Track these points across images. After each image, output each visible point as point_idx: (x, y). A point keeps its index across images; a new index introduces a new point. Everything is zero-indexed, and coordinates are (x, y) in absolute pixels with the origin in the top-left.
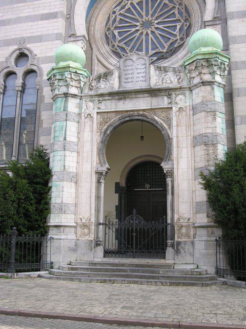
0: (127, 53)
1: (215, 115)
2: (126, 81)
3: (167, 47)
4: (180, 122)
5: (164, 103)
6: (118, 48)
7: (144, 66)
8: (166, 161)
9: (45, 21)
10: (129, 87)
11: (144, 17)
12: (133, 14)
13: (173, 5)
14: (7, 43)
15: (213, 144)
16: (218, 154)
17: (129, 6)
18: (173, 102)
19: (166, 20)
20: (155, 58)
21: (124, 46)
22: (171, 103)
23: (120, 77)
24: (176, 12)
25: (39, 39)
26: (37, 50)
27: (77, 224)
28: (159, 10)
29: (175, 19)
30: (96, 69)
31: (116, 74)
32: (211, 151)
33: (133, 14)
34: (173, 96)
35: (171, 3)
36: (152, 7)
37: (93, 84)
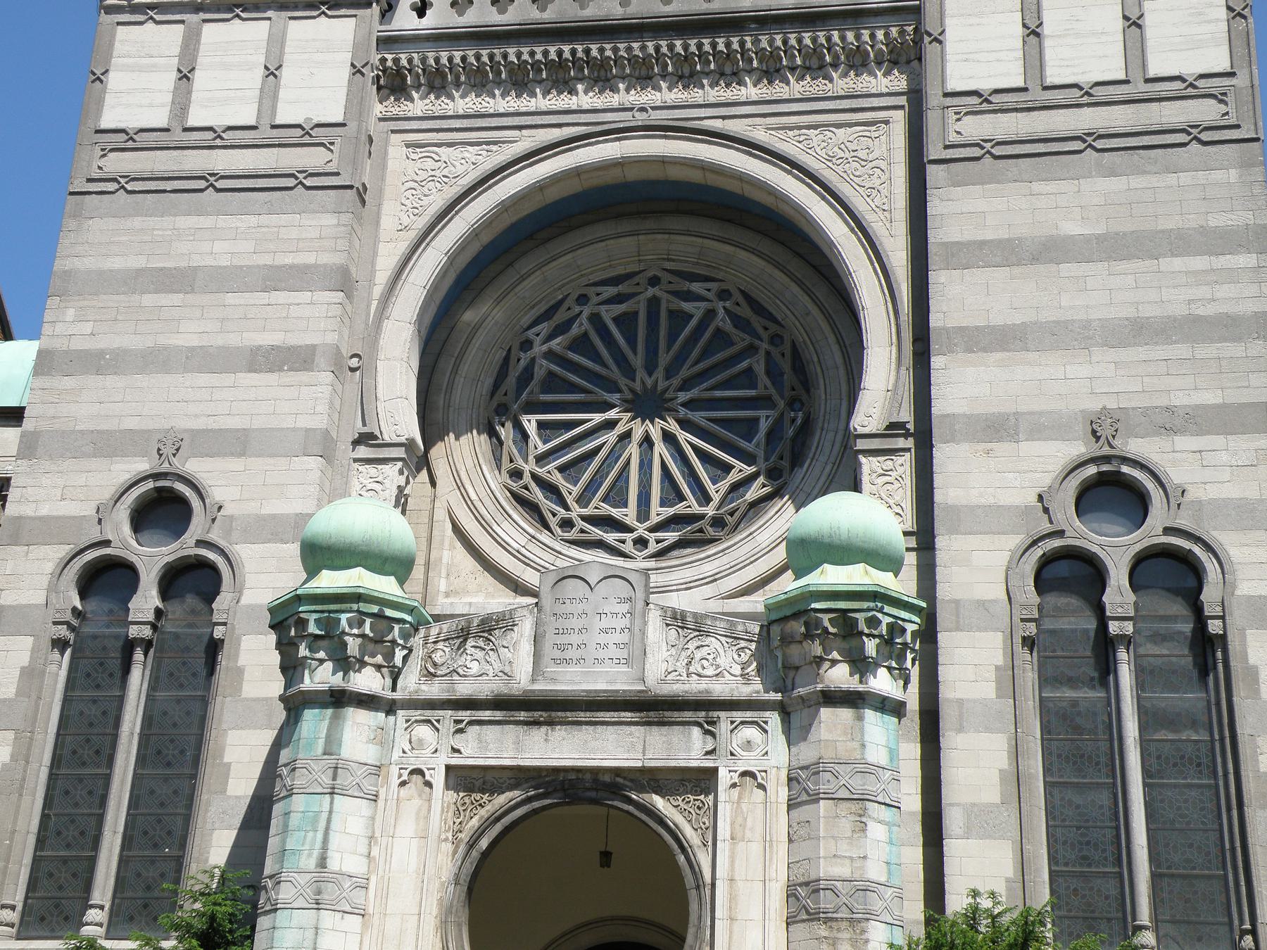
0: (567, 508)
1: (862, 814)
2: (557, 654)
3: (716, 498)
4: (743, 826)
5: (689, 750)
6: (533, 485)
7: (625, 607)
9: (262, 375)
10: (571, 680)
11: (641, 374)
12: (597, 358)
13: (748, 339)
14: (107, 444)
15: (851, 920)
17: (586, 325)
18: (721, 751)
20: (671, 536)
21: (558, 479)
23: (537, 640)
24: (760, 369)
25: (237, 443)
26: (226, 485)
28: (696, 353)
29: (753, 393)
30: (444, 561)
31: (526, 627)
33: (597, 358)
34: (724, 727)
36: (672, 338)
37: (437, 657)
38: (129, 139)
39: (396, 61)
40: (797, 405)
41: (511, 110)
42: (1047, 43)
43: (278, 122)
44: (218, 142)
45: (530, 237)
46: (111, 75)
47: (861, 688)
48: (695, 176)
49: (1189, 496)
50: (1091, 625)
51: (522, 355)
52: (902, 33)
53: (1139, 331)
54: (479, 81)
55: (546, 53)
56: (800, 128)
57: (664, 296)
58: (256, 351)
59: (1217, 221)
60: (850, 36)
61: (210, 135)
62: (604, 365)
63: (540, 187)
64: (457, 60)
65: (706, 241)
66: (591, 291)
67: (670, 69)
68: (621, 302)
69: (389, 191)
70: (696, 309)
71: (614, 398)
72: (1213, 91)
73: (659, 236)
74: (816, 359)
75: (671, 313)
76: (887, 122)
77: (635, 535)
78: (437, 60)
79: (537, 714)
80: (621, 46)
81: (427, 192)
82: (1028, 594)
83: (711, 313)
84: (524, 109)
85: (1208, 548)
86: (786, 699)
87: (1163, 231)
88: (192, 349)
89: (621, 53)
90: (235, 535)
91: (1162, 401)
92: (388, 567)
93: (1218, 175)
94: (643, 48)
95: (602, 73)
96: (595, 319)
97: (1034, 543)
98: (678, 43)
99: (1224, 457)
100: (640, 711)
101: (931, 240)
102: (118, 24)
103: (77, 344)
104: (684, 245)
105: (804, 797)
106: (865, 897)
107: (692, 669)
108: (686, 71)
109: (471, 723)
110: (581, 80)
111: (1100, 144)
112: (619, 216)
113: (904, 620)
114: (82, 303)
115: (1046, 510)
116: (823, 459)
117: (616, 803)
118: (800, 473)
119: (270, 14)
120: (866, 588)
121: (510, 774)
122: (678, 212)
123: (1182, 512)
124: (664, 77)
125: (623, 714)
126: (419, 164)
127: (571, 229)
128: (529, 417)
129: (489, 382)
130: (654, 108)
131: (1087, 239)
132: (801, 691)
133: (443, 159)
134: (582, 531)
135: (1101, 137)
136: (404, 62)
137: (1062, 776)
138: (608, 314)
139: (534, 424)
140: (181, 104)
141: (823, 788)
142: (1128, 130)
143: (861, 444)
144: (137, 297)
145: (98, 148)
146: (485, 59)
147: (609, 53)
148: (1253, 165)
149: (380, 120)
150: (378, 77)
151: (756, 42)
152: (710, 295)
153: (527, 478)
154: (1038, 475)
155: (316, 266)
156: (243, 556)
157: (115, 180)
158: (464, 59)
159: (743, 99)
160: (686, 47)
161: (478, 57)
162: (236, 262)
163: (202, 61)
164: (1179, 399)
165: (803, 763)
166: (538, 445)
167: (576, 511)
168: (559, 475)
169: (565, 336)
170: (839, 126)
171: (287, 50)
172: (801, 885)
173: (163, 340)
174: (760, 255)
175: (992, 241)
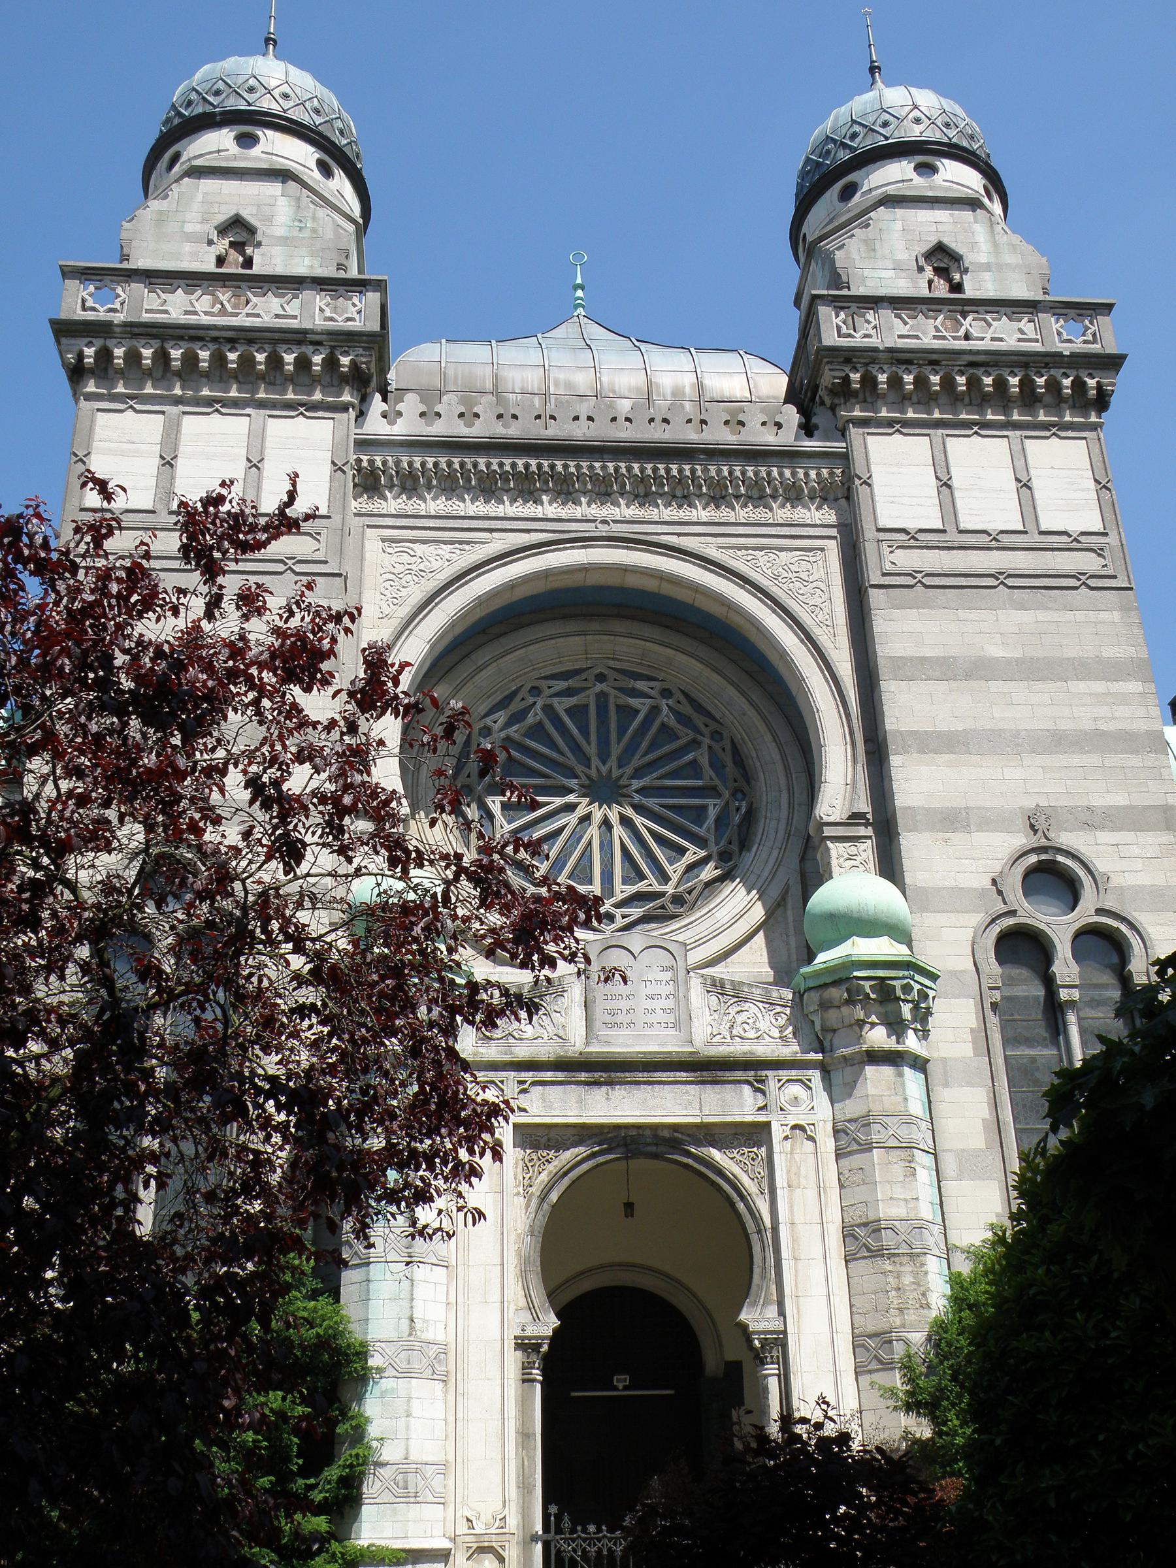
2: (608, 1019)
3: (675, 878)
4: (798, 1174)
5: (742, 1106)
7: (668, 975)
8: (754, 1304)
11: (595, 762)
12: (553, 745)
13: (692, 735)
15: (911, 1255)
16: (929, 1289)
18: (772, 1107)
19: (668, 782)
20: (636, 912)
22: (764, 1108)
24: (704, 761)
27: (454, 1540)
28: (644, 745)
29: (699, 783)
32: (907, 1280)
33: (553, 745)
34: (772, 1085)
35: (685, 726)
36: (622, 731)
40: (739, 796)
41: (481, 514)
42: (957, 494)
45: (483, 631)
47: (900, 1048)
50: (1040, 992)
52: (832, 474)
53: (1059, 741)
54: (450, 485)
55: (514, 465)
56: (747, 549)
57: (613, 692)
59: (1108, 653)
60: (787, 473)
62: (562, 753)
63: (512, 586)
64: (430, 465)
65: (648, 644)
66: (544, 684)
67: (628, 488)
69: (368, 582)
70: (642, 706)
71: (573, 783)
75: (618, 706)
76: (822, 550)
78: (410, 464)
79: (597, 1075)
80: (584, 464)
81: (406, 584)
82: (992, 966)
83: (655, 710)
84: (493, 514)
86: (828, 1060)
87: (1068, 659)
89: (585, 470)
93: (1105, 615)
94: (604, 468)
95: (565, 487)
96: (548, 709)
97: (993, 921)
98: (636, 466)
100: (694, 1071)
101: (879, 654)
102: (98, 410)
104: (628, 646)
105: (855, 1147)
106: (921, 1234)
107: (735, 1032)
108: (642, 491)
109: (534, 1084)
110: (546, 491)
111: (1010, 582)
112: (565, 617)
113: (927, 987)
115: (1000, 893)
116: (769, 844)
117: (675, 1157)
118: (748, 857)
119: (248, 411)
120: (900, 959)
121: (571, 1131)
122: (619, 616)
123: (1109, 896)
124: (622, 495)
125: (678, 1074)
126: (395, 558)
127: (521, 626)
128: (493, 798)
130: (615, 522)
131: (1009, 661)
132: (846, 1051)
133: (419, 554)
135: (1010, 576)
136: (379, 464)
137: (1027, 1124)
138: (561, 705)
139: (499, 805)
141: (875, 1138)
142: (1031, 572)
143: (828, 831)
146: (457, 466)
147: (572, 470)
148: (1130, 609)
151: (706, 470)
152: (652, 693)
158: (436, 465)
160: (642, 470)
161: (449, 464)
164: (1097, 801)
165: (849, 1117)
169: (522, 724)
170: (781, 549)
171: (267, 444)
172: (858, 1226)
175: (930, 658)
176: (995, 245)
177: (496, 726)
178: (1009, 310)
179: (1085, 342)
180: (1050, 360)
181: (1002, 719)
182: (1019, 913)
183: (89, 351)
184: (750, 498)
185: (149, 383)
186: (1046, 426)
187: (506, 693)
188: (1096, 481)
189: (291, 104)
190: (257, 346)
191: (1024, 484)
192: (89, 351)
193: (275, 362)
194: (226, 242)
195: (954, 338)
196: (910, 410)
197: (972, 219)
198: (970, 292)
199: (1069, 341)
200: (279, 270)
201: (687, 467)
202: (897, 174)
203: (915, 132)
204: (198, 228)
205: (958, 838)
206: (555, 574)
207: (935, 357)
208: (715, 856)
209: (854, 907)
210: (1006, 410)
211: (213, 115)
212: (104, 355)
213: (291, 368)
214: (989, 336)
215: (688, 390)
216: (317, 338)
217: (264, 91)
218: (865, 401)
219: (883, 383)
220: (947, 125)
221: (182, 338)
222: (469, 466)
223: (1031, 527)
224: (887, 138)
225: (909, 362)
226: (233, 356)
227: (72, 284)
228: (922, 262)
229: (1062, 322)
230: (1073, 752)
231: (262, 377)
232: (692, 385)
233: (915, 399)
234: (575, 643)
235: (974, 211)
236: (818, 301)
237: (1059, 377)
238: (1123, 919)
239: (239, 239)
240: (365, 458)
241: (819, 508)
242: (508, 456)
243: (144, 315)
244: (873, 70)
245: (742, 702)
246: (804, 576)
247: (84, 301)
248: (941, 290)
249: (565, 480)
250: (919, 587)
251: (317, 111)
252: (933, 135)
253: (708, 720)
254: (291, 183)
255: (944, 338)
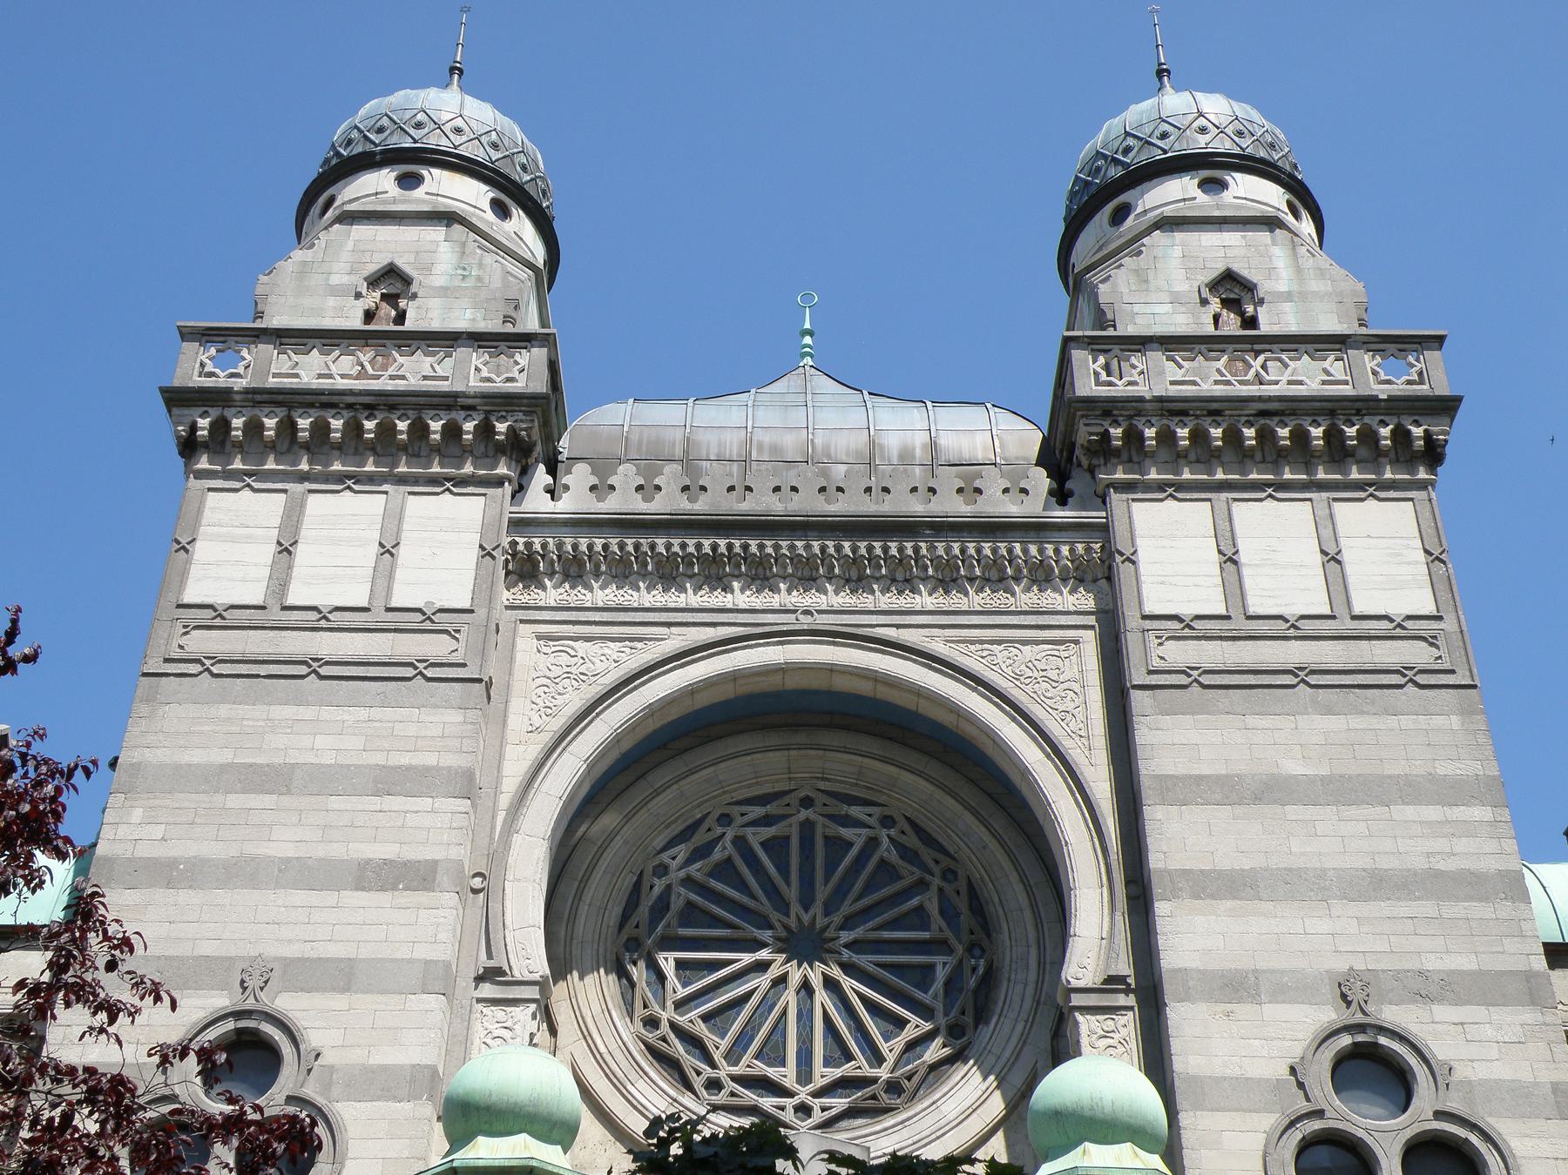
0: (713, 1065)
3: (891, 1058)
6: (672, 1037)
11: (795, 908)
12: (743, 887)
13: (918, 873)
17: (730, 849)
19: (886, 935)
20: (839, 1103)
21: (701, 1029)
24: (933, 907)
25: (341, 976)
29: (926, 935)
33: (743, 887)
36: (830, 869)
38: (217, 617)
39: (528, 545)
40: (977, 952)
42: (1245, 572)
43: (393, 604)
44: (323, 623)
45: (664, 746)
46: (198, 544)
48: (864, 688)
49: (1458, 1075)
51: (656, 881)
52: (1088, 550)
53: (1377, 884)
54: (622, 571)
55: (699, 546)
56: (982, 642)
58: (364, 865)
59: (1444, 769)
60: (1033, 549)
61: (314, 615)
62: (753, 897)
63: (692, 691)
64: (598, 548)
65: (867, 760)
67: (837, 571)
68: (769, 825)
69: (517, 687)
71: (766, 935)
72: (1423, 633)
73: (813, 752)
74: (996, 900)
75: (826, 838)
76: (1076, 642)
77: (796, 1101)
78: (575, 547)
80: (784, 544)
83: (873, 842)
84: (673, 605)
85: (1487, 1137)
87: (1390, 777)
88: (288, 860)
89: (784, 551)
90: (336, 1091)
91: (1413, 964)
92: (555, 1135)
93: (1439, 721)
94: (808, 547)
95: (760, 570)
96: (740, 842)
97: (1292, 1124)
98: (847, 545)
99: (1489, 1032)
101: (1143, 771)
102: (210, 490)
103: (143, 851)
110: (737, 577)
111: (1313, 680)
114: (152, 802)
115: (1301, 1085)
118: (986, 1032)
119: (385, 487)
123: (1453, 1093)
124: (829, 579)
126: (551, 659)
128: (666, 954)
129: (616, 911)
131: (1312, 780)
134: (733, 1094)
135: (1313, 672)
136: (537, 547)
138: (756, 837)
139: (672, 963)
140: (280, 579)
143: (1076, 1000)
144: (219, 798)
145: (179, 624)
146: (630, 549)
147: (770, 550)
148: (1473, 713)
149: (507, 607)
150: (507, 561)
151: (932, 548)
152: (871, 821)
153: (665, 1028)
154: (1288, 1044)
155: (438, 768)
156: (346, 1117)
157: (198, 661)
158: (605, 547)
159: (918, 608)
160: (855, 549)
161: (622, 546)
162: (342, 760)
163: (305, 533)
164: (1432, 963)
166: (677, 988)
167: (725, 1071)
168: (703, 1025)
169: (707, 861)
170: (1025, 643)
173: (250, 849)
174: (928, 779)
176: (1299, 270)
177: (674, 864)
178: (1310, 347)
179: (1409, 382)
180: (1363, 406)
181: (1303, 854)
182: (1327, 1114)
183: (203, 423)
184: (988, 580)
185: (271, 458)
186: (1360, 486)
187: (690, 821)
188: (1427, 552)
189: (464, 138)
190: (399, 413)
191: (1332, 558)
192: (203, 423)
193: (419, 430)
194: (377, 295)
195: (1240, 382)
196: (1186, 470)
197: (1269, 241)
198: (1266, 327)
199: (1388, 382)
200: (436, 324)
201: (909, 545)
202: (1177, 192)
203: (1201, 143)
204: (345, 279)
205: (1244, 1010)
206: (745, 676)
207: (1215, 406)
208: (943, 1031)
209: (1086, 1102)
210: (1309, 467)
211: (373, 154)
212: (221, 427)
213: (437, 437)
214: (1285, 379)
215: (918, 452)
216: (470, 401)
217: (433, 126)
218: (1130, 461)
219: (1151, 439)
220: (1240, 134)
221: (311, 405)
222: (645, 548)
223: (1341, 611)
224: (1165, 152)
225: (1184, 413)
226: (369, 425)
227: (191, 347)
228: (1206, 293)
229: (1378, 359)
230: (1399, 899)
231: (404, 448)
232: (924, 446)
233: (1192, 457)
234: (776, 759)
235: (1272, 231)
236: (1072, 344)
237: (1375, 427)
238: (1473, 1127)
239: (393, 290)
240: (521, 540)
241: (1073, 591)
242: (692, 536)
243: (271, 380)
244: (1161, 73)
245: (982, 831)
246: (1053, 674)
247: (202, 365)
248: (1231, 325)
249: (760, 563)
250: (1196, 688)
251: (495, 146)
252: (1224, 145)
253: (940, 856)
254: (457, 227)
255: (1228, 383)
